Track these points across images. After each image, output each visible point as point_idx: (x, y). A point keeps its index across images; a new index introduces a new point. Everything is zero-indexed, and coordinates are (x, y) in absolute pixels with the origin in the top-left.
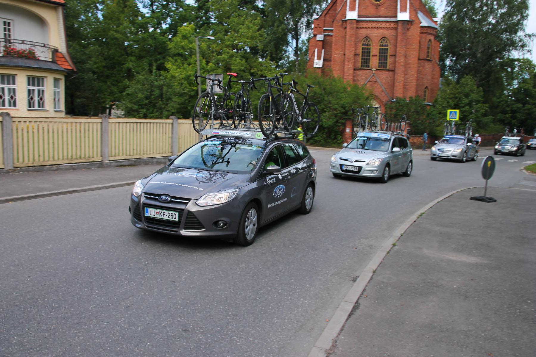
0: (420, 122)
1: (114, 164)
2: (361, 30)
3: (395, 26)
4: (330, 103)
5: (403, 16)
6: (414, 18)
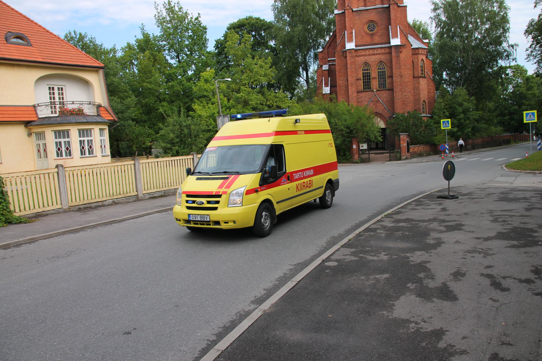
0: (418, 133)
1: (148, 197)
2: (360, 57)
3: (390, 51)
4: (336, 125)
5: (395, 42)
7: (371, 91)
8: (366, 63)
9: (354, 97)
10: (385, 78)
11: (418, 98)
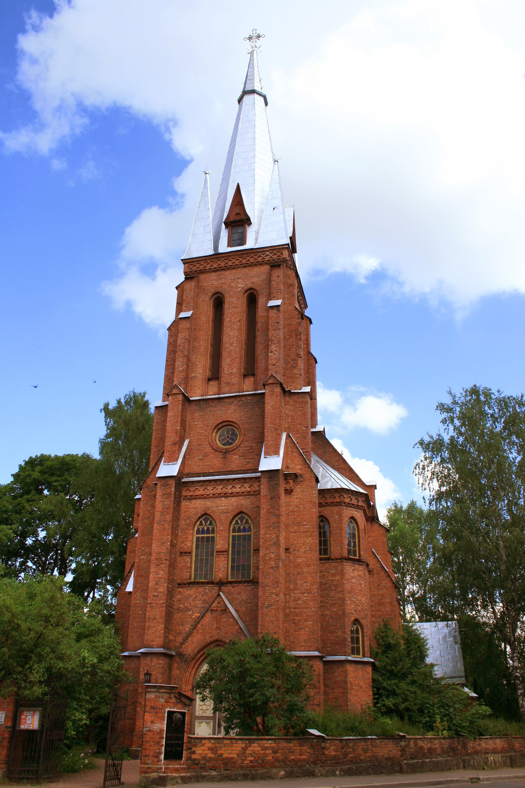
2: (193, 501)
6: (300, 469)
8: (206, 514)
9: (160, 595)
11: (340, 613)
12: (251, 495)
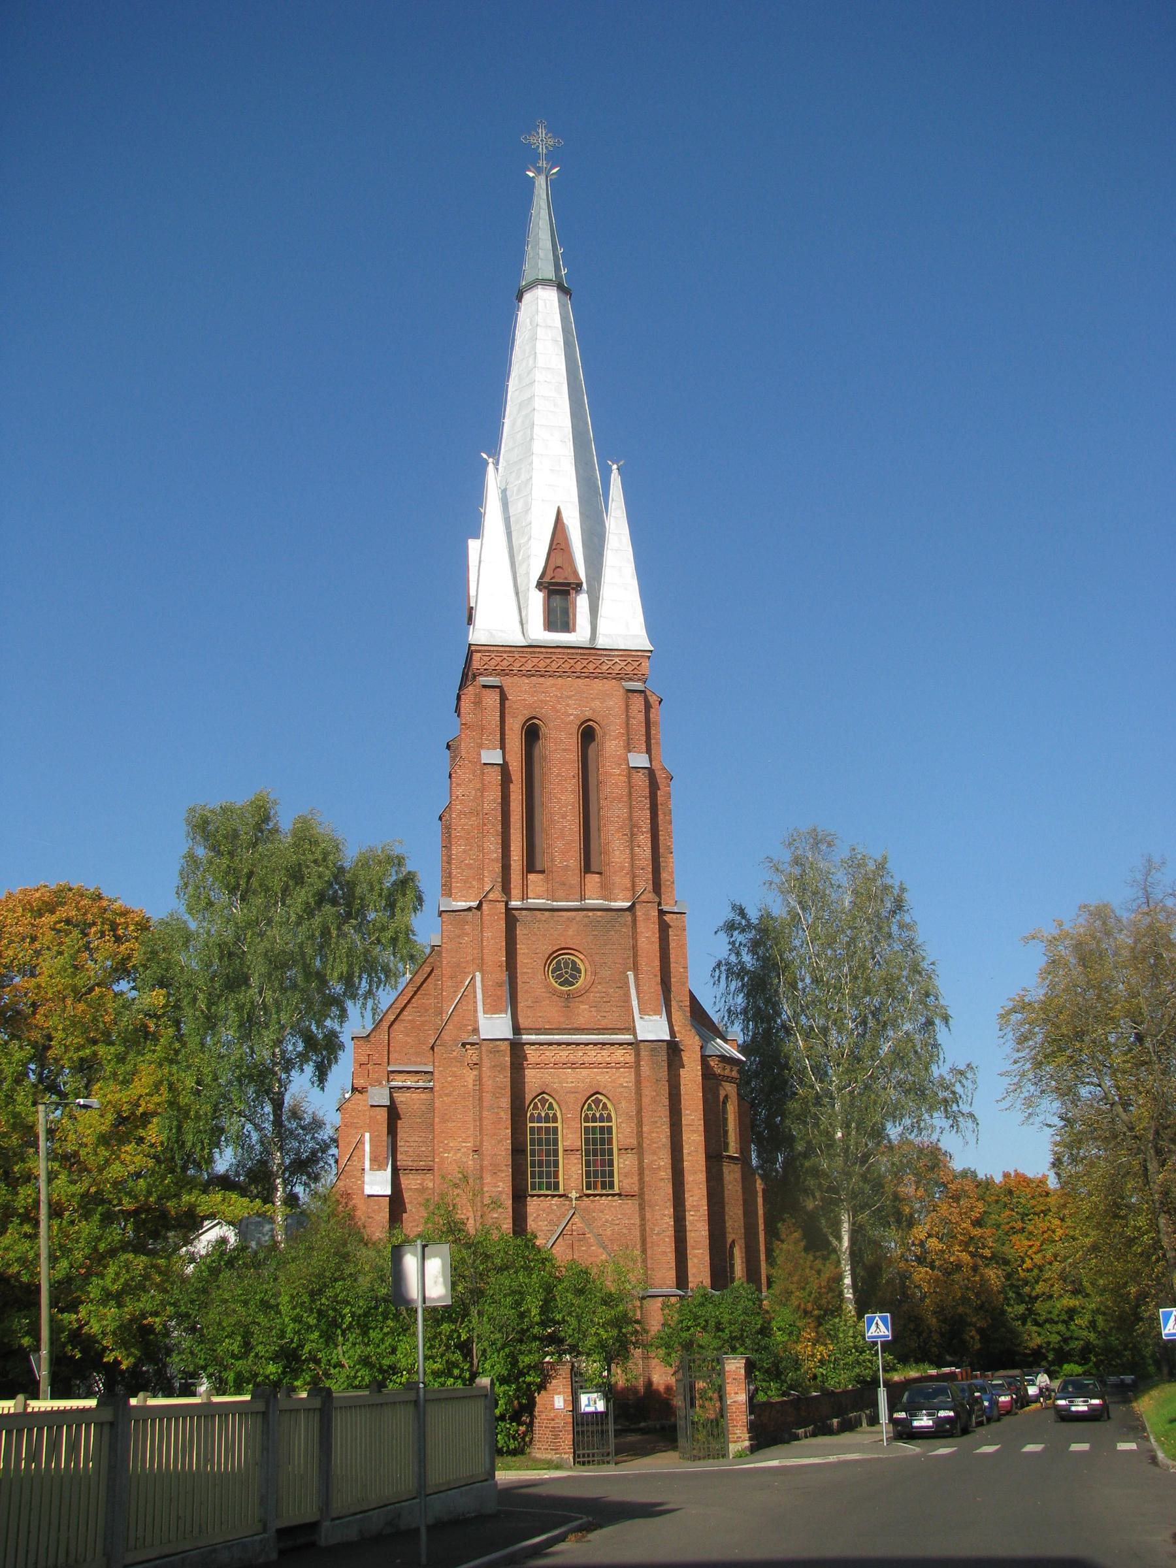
7: (560, 1196)
10: (611, 1153)
12: (612, 1067)
